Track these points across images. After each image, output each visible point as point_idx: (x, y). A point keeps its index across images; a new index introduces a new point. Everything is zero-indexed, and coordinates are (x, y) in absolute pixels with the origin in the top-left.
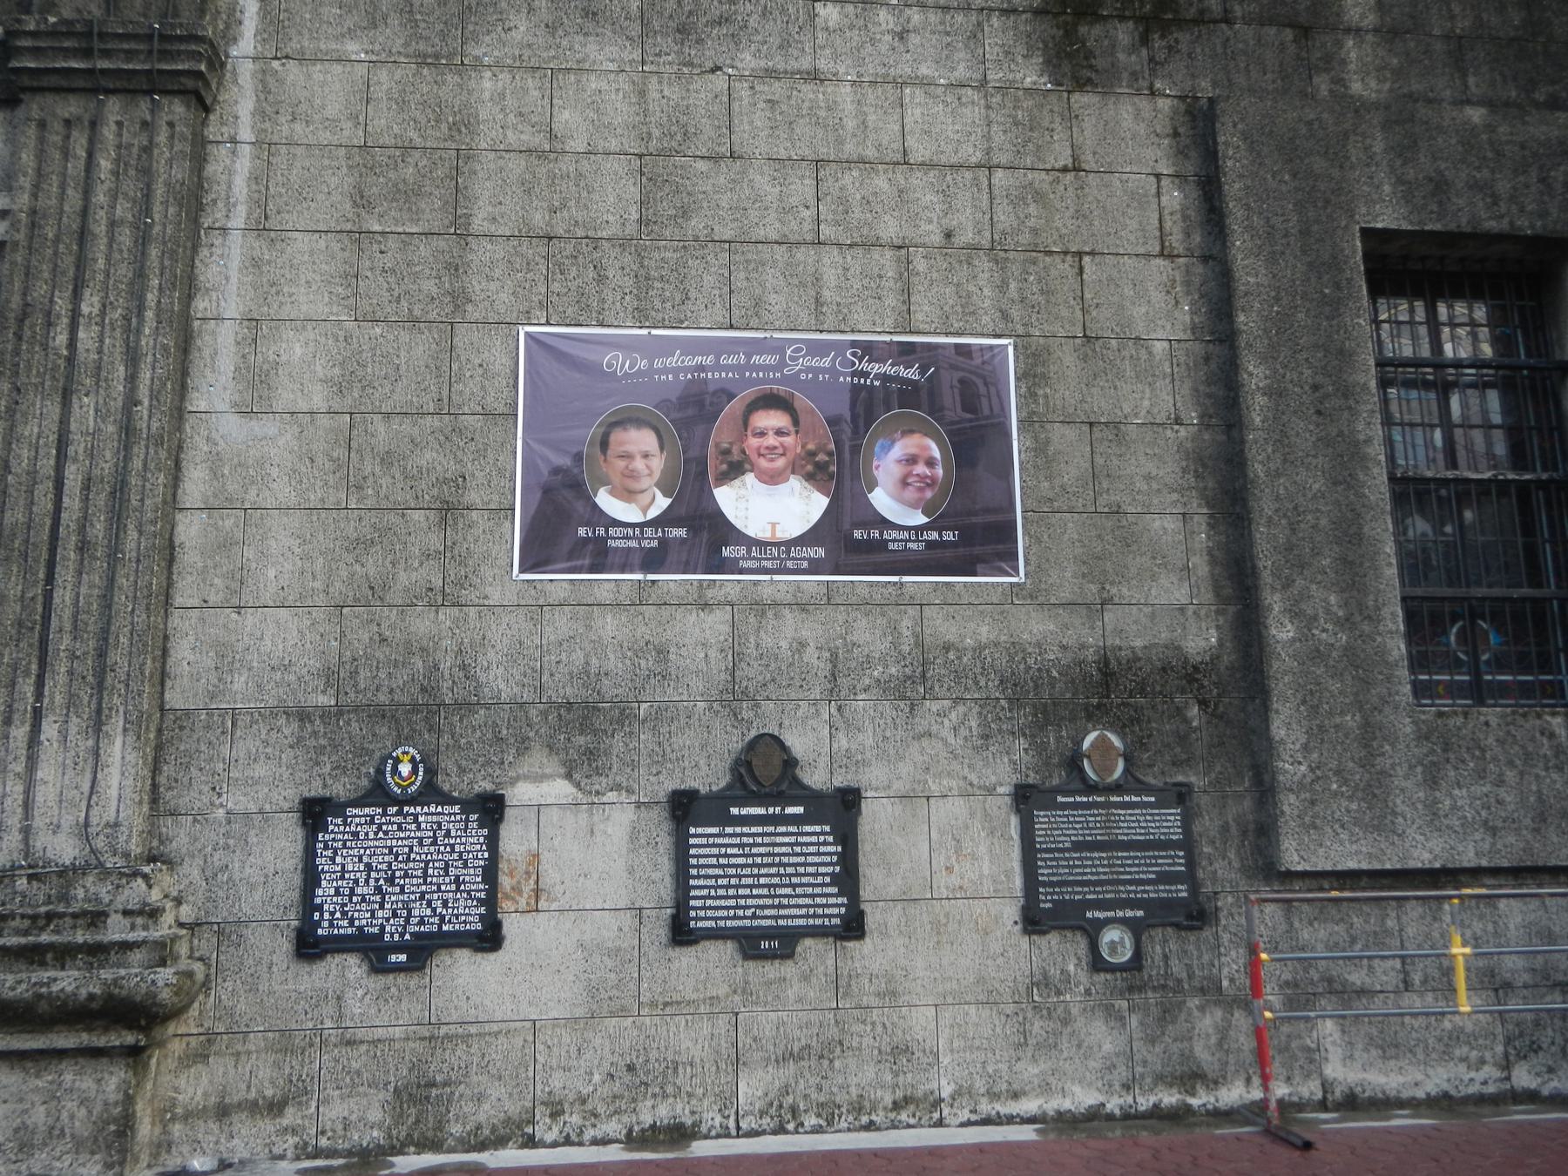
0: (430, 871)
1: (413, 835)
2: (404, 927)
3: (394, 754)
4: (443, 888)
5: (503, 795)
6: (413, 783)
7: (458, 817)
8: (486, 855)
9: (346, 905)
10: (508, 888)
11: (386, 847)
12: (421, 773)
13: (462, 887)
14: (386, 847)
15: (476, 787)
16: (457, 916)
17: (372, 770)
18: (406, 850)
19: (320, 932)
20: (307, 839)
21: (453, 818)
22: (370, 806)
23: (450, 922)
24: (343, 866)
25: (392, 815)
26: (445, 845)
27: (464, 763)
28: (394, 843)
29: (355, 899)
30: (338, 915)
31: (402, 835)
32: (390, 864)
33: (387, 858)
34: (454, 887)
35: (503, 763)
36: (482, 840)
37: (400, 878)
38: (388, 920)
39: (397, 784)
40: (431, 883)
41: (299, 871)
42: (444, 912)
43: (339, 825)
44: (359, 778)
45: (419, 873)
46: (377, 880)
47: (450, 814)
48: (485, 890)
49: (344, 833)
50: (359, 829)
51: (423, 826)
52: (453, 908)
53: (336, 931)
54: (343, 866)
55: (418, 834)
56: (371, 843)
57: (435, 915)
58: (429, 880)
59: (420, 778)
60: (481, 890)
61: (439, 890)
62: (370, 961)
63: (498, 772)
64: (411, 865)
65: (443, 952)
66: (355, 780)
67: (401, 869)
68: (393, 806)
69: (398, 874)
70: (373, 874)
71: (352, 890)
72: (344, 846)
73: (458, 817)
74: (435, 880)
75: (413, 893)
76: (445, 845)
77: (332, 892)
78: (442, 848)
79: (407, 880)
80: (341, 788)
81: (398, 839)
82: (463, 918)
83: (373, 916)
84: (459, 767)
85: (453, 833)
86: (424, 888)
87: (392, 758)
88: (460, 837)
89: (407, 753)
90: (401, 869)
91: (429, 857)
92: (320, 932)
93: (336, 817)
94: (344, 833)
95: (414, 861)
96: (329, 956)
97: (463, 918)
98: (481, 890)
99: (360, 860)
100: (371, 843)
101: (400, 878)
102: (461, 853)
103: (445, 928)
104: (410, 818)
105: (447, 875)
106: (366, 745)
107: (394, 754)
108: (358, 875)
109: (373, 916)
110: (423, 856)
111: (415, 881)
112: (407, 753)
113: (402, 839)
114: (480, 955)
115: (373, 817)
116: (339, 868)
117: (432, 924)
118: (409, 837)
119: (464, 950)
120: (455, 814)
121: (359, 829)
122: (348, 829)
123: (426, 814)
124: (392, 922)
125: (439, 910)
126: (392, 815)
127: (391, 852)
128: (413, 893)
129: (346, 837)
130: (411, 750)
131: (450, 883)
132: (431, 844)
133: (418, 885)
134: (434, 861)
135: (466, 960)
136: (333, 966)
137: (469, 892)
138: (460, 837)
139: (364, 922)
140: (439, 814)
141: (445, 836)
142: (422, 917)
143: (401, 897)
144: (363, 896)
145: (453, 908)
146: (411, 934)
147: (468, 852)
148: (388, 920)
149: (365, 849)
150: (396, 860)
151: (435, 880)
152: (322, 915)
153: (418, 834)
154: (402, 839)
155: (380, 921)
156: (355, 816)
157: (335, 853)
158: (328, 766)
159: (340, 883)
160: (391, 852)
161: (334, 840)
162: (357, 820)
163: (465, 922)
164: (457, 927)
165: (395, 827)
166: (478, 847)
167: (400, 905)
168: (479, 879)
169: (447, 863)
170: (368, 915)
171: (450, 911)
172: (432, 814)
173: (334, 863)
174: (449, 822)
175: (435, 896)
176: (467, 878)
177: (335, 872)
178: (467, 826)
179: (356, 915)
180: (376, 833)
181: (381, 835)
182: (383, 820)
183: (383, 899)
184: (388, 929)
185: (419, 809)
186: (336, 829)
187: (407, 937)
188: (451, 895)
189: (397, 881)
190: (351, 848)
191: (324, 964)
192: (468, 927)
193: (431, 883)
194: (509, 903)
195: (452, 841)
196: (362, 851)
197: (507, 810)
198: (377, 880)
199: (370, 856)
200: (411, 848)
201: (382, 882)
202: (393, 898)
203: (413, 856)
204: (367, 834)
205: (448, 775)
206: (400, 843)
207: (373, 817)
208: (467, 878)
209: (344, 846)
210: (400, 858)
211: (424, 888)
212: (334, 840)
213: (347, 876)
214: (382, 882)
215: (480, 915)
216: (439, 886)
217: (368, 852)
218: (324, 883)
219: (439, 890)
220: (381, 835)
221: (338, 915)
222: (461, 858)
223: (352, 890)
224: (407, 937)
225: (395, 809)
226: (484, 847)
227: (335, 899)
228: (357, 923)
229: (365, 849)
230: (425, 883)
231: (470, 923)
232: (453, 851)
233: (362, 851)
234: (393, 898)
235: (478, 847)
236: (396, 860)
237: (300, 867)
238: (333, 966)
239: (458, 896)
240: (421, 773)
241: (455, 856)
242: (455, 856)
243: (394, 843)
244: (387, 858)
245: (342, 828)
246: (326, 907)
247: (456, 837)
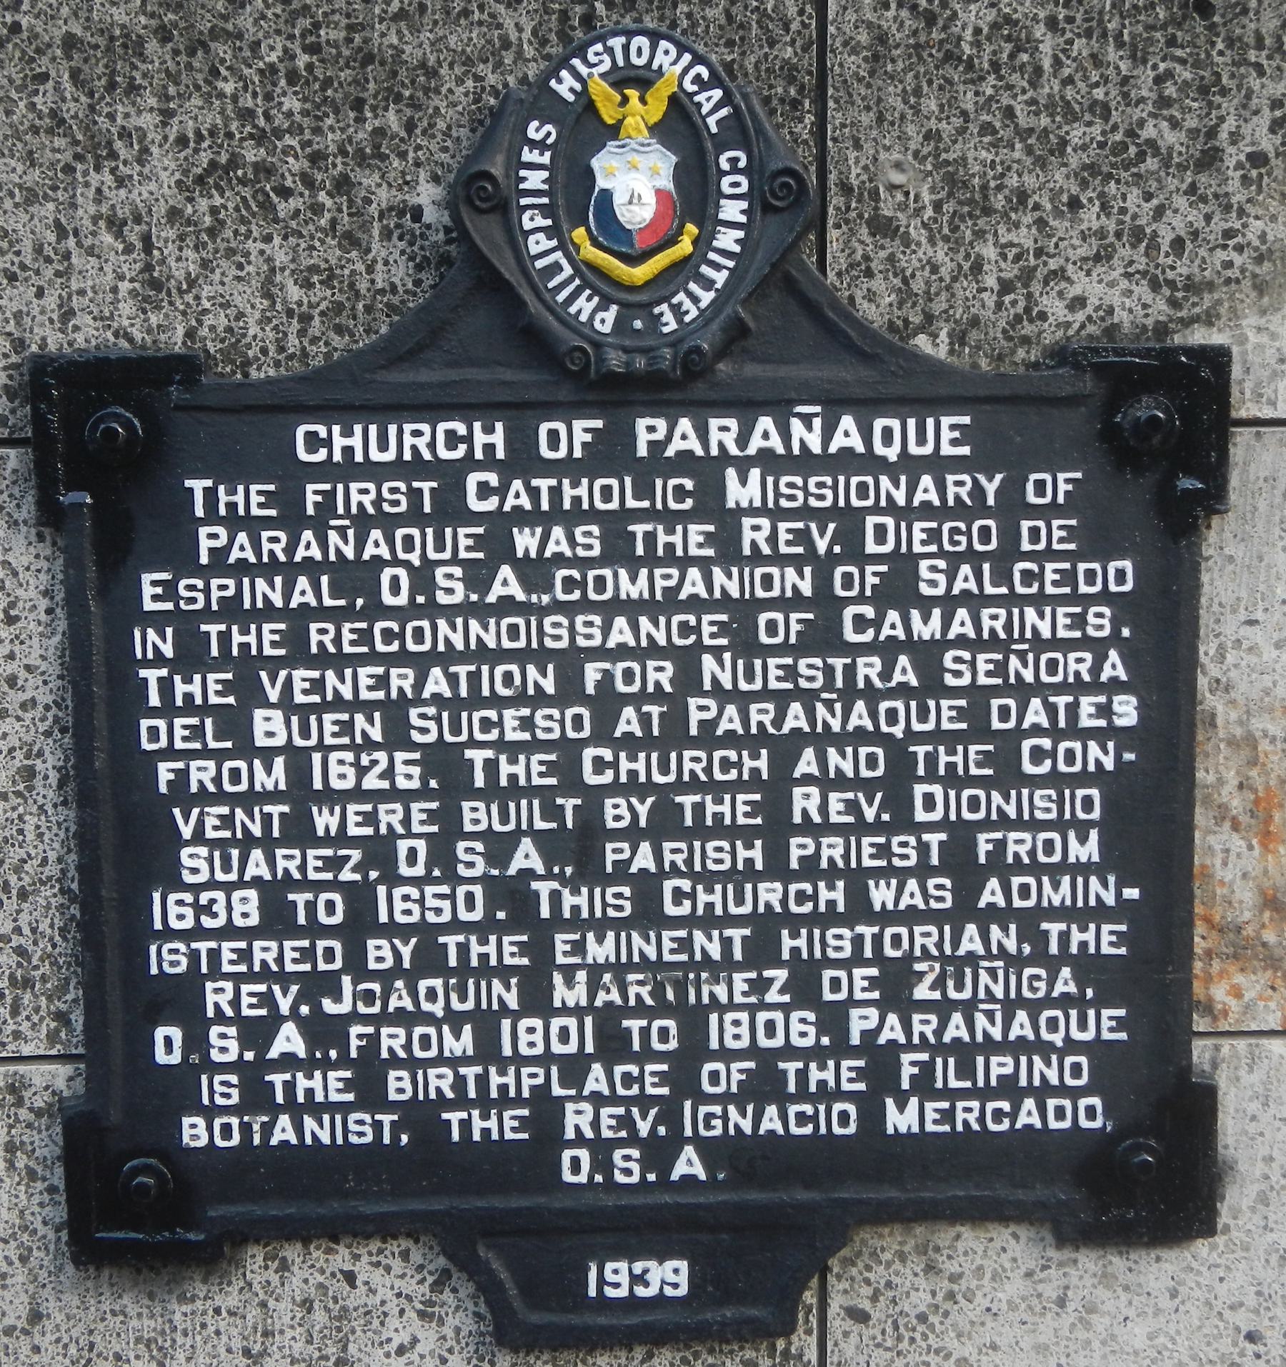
0: (805, 801)
1: (694, 584)
2: (671, 1113)
3: (565, 86)
4: (881, 895)
5: (1218, 359)
6: (682, 271)
7: (959, 487)
8: (1127, 711)
9: (328, 985)
10: (1246, 896)
11: (540, 656)
12: (732, 210)
13: (992, 893)
14: (540, 656)
15: (1055, 307)
16: (964, 1054)
17: (427, 194)
18: (662, 674)
19: (194, 1131)
20: (74, 603)
21: (927, 490)
22: (432, 410)
23: (924, 1086)
24: (298, 760)
25: (569, 468)
26: (888, 651)
27: (977, 155)
28: (589, 631)
29: (379, 952)
30: (289, 1040)
31: (634, 588)
32: (568, 751)
33: (548, 723)
34: (942, 891)
35: (1209, 159)
36: (1100, 622)
37: (633, 834)
38: (574, 1069)
39: (591, 277)
40: (810, 868)
41: (46, 792)
42: (893, 1030)
43: (253, 526)
44: (350, 241)
45: (740, 808)
46: (500, 846)
47: (910, 467)
48: (1123, 909)
49: (290, 570)
50: (376, 545)
51: (754, 533)
52: (943, 1009)
53: (284, 1131)
54: (298, 760)
55: (727, 582)
56: (450, 634)
57: (841, 1049)
58: (799, 847)
59: (728, 240)
60: (1100, 913)
61: (859, 909)
62: (488, 1289)
63: (1183, 216)
64: (692, 762)
65: (889, 1241)
66: (331, 252)
67: (633, 787)
68: (569, 411)
69: (615, 812)
70: (475, 815)
71: (359, 898)
72: (298, 652)
73: (959, 487)
74: (833, 849)
75: (709, 921)
76: (888, 651)
77: (247, 907)
78: (869, 667)
79: (673, 852)
80: (246, 298)
81: (617, 606)
82: (1001, 1066)
83: (487, 1051)
84: (954, 182)
85: (931, 580)
86: (770, 893)
87: (546, 103)
88: (974, 601)
89: (643, 80)
90: (633, 787)
91: (796, 717)
92: (194, 1131)
93: (232, 473)
94: (290, 570)
95: (708, 737)
96: (255, 1257)
97: (1001, 1066)
98: (1100, 913)
99: (397, 737)
100: (450, 634)
101: (633, 834)
102: (978, 695)
103: (900, 1119)
104: (665, 490)
105: (903, 821)
106: (386, 38)
107: (565, 86)
108: (390, 816)
109: (487, 1051)
110: (762, 714)
111: (717, 854)
112: (643, 80)
113: (632, 609)
114: (1088, 1261)
115: (451, 476)
116: (276, 777)
117: (827, 1094)
118: (670, 602)
119: (1002, 1235)
120: (938, 465)
121: (376, 545)
122: (308, 547)
123: (766, 459)
124: (596, 1079)
125: (860, 1022)
126: (569, 468)
127: (570, 690)
128: (709, 921)
129: (303, 594)
130: (666, 57)
131: (923, 871)
132: (802, 648)
133: (742, 876)
134: (823, 739)
135: (1015, 1287)
136: (284, 1311)
137: (1029, 923)
138: (974, 601)
139: (440, 1081)
140: (845, 462)
141: (885, 597)
142: (766, 1061)
143: (641, 945)
144: (426, 933)
145: (943, 1009)
146: (706, 1148)
147: (1023, 691)
148: (574, 1069)
149: (422, 664)
150: (602, 734)
151: (833, 849)
152: (196, 1041)
153: (727, 582)
154: (632, 609)
155: (531, 1078)
156: (349, 469)
157: (251, 695)
158: (165, 166)
159: (288, 861)
160: (570, 690)
161: (231, 610)
162: (361, 495)
163: (1009, 1088)
164: (967, 1114)
165: (590, 539)
166: (1078, 664)
167: (639, 990)
168: (1088, 850)
169: (899, 753)
170: (462, 1044)
171: (924, 1025)
172: (805, 463)
173: (246, 749)
174: (906, 514)
175: (840, 941)
176: (1019, 844)
177: (250, 799)
178: (1010, 536)
179: (392, 1040)
180: (478, 577)
181: (506, 583)
182: (518, 497)
183: (540, 950)
184: (577, 1118)
185: (723, 431)
186: (242, 550)
187: (688, 1164)
188: (926, 936)
189: (612, 853)
190: (339, 661)
191: (231, 1299)
192: (1028, 1115)
193: (810, 868)
194: (1253, 984)
195: (927, 628)
196: (402, 679)
197: (1241, 440)
198: (500, 846)
199: (452, 705)
200: (687, 662)
201: (527, 857)
202: (599, 951)
203: (698, 711)
204: (423, 577)
205: (882, 227)
206: (621, 633)
207: (451, 476)
208: (1019, 844)
209: (296, 643)
210: (628, 723)
211: (770, 893)
212: (231, 610)
213: (325, 821)
214: (527, 857)
215: (1096, 1048)
216: (857, 880)
217: (436, 683)
218: (194, 861)
219: (859, 909)
220: (506, 583)
221: (289, 1040)
222: (980, 731)
223: (359, 898)
224: (688, 1164)
225: (582, 430)
226: (1114, 667)
227: (265, 951)
228: (398, 1084)
229: (422, 664)
230: (777, 868)
231: (1043, 1092)
232: (932, 685)
233: (402, 679)
234: (599, 951)
235: (1078, 664)
236: (602, 734)
237: (49, 765)
238: (284, 1311)
239: (971, 941)
240: (732, 210)
241: (946, 714)
242: (946, 714)
243: (589, 631)
244: (548, 723)
245: (274, 543)
246: (217, 996)
247: (949, 603)
